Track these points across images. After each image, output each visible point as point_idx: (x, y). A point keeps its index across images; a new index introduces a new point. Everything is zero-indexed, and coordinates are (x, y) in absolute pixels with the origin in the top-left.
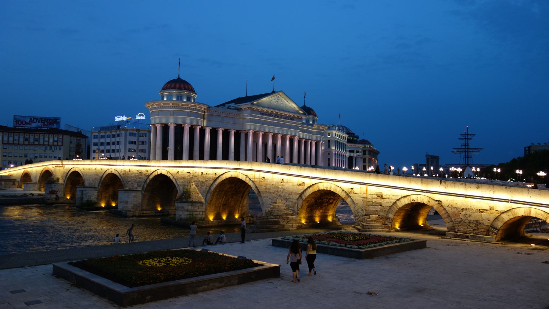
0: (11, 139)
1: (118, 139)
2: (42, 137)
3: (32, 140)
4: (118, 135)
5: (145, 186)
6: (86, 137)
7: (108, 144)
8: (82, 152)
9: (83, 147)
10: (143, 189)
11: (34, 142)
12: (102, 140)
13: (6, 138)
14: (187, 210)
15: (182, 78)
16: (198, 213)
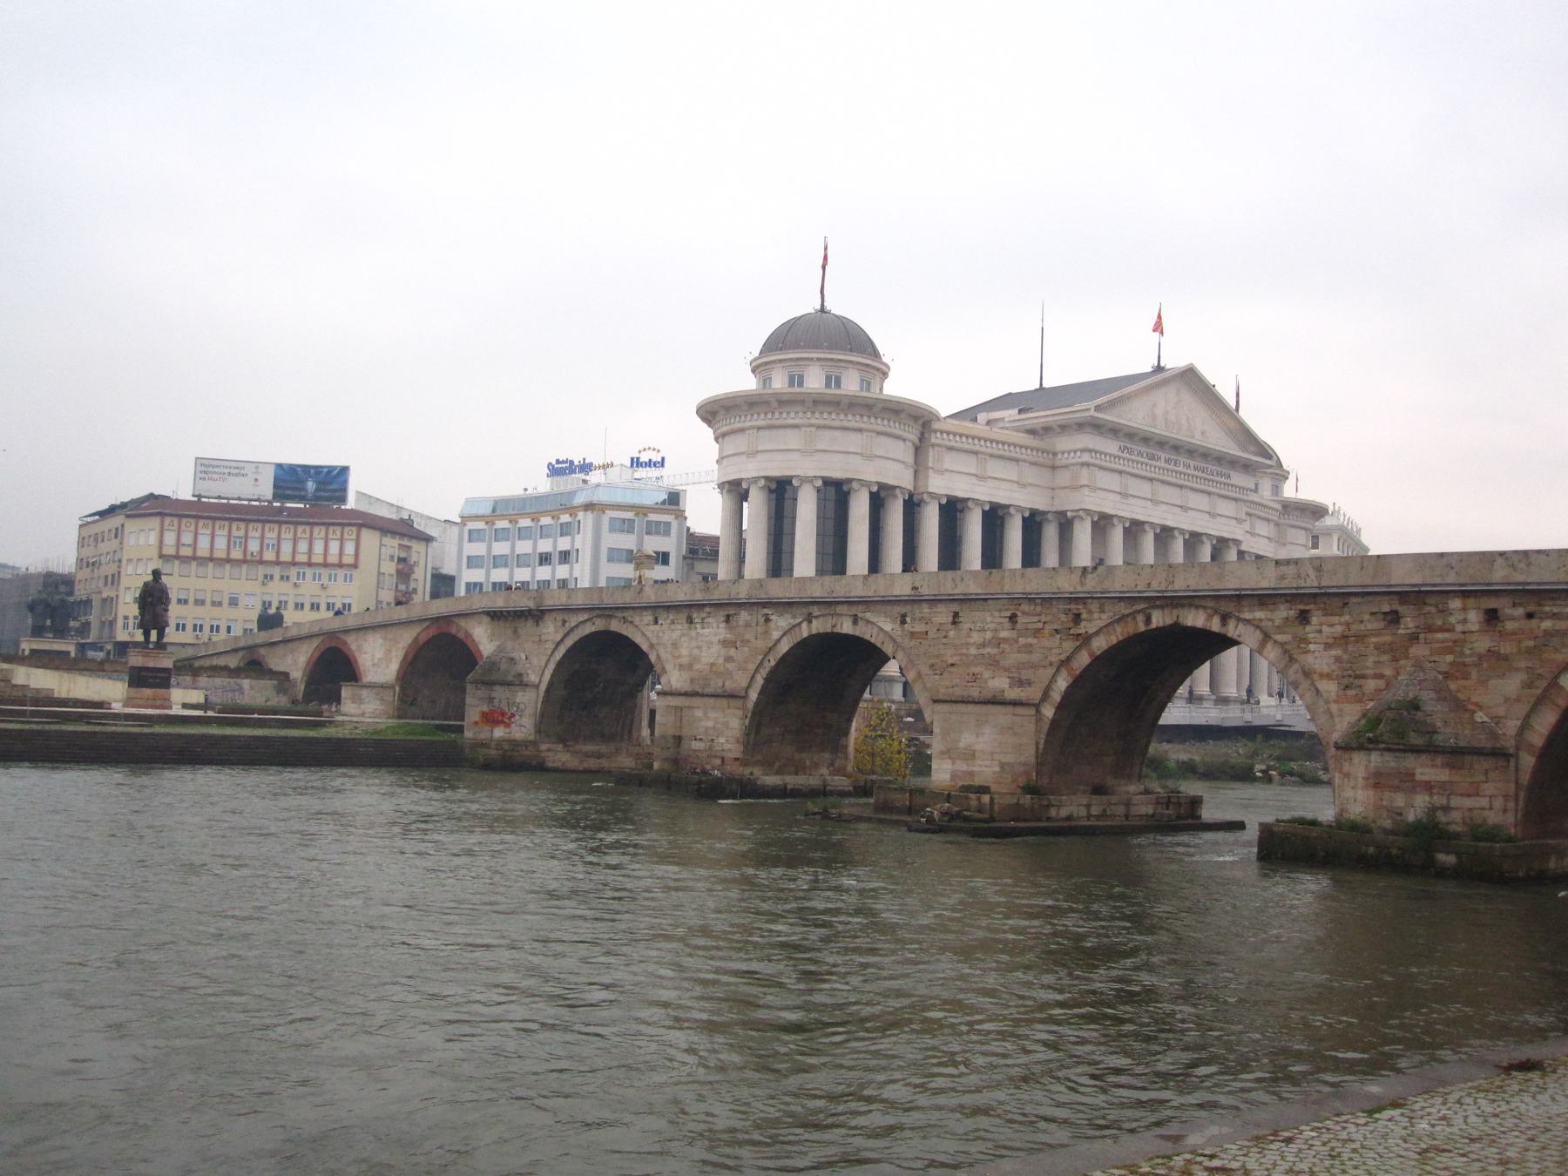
0: (187, 538)
1: (564, 544)
2: (287, 535)
3: (254, 546)
4: (565, 530)
5: (1062, 684)
6: (428, 539)
7: (545, 559)
8: (415, 591)
9: (419, 573)
10: (1046, 695)
11: (261, 552)
12: (501, 548)
13: (170, 538)
14: (1428, 787)
15: (836, 307)
16: (1484, 802)
